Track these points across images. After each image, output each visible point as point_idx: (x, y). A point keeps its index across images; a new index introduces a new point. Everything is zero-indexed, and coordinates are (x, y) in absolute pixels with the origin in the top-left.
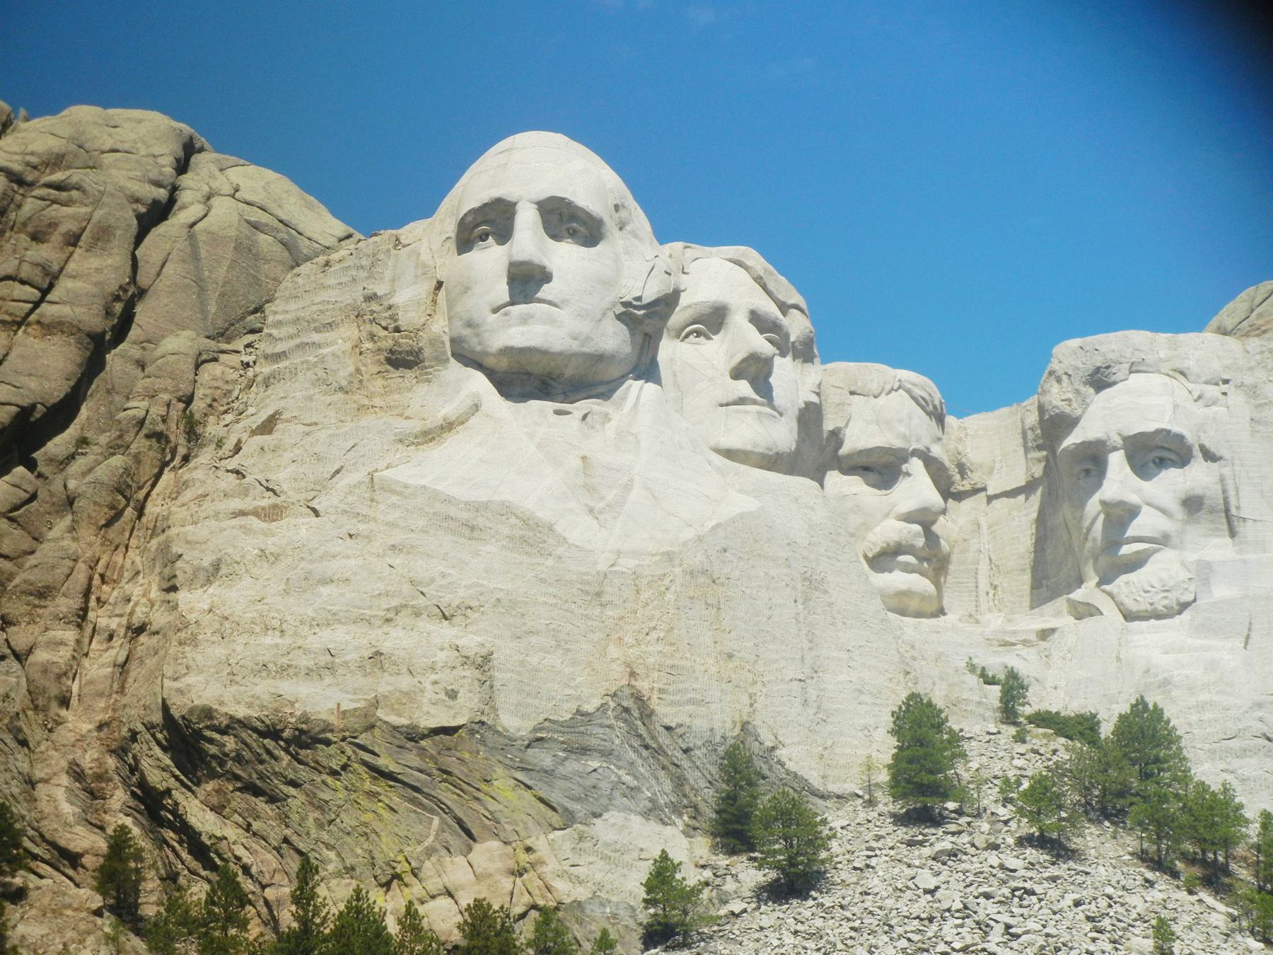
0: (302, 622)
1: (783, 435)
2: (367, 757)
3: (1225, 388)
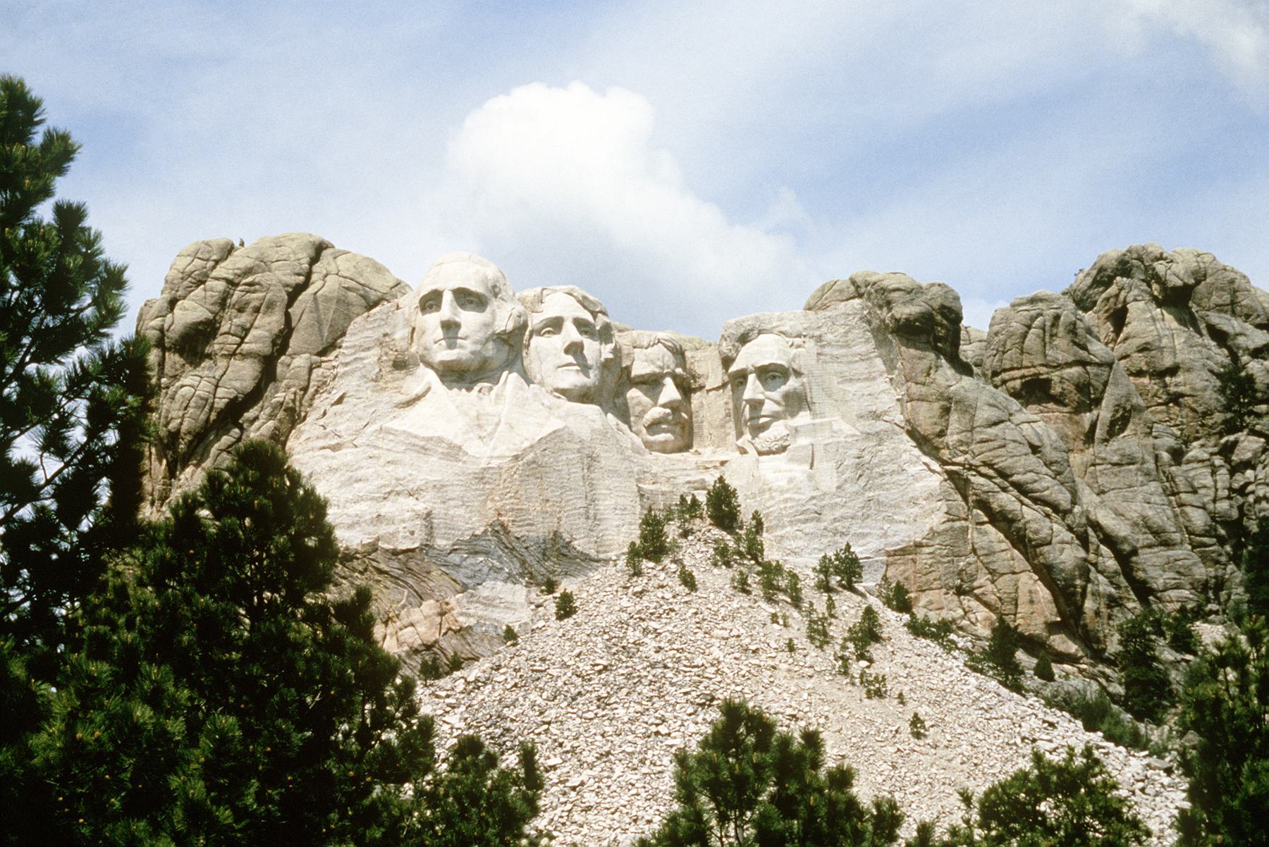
1: (592, 379)
2: (375, 564)
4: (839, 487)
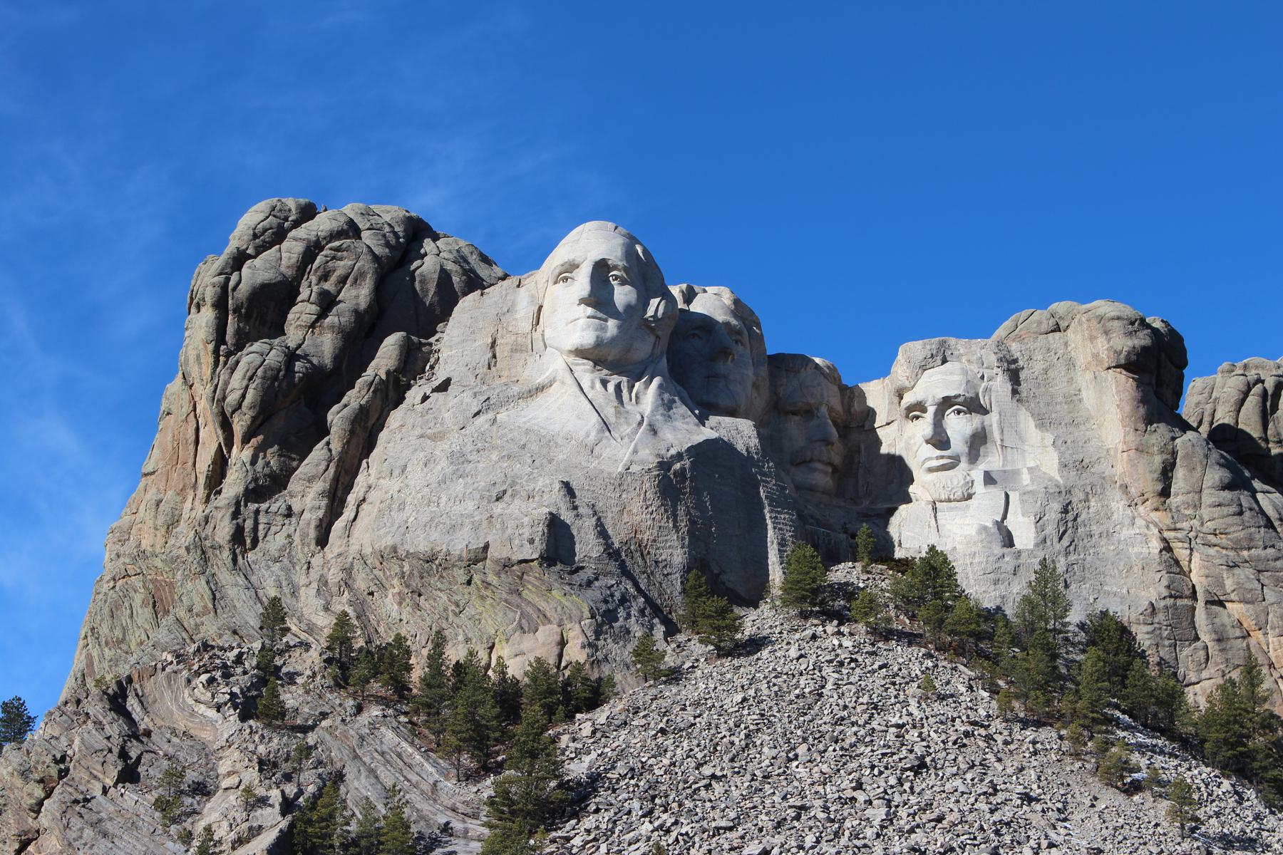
3: (996, 370)
4: (1037, 545)
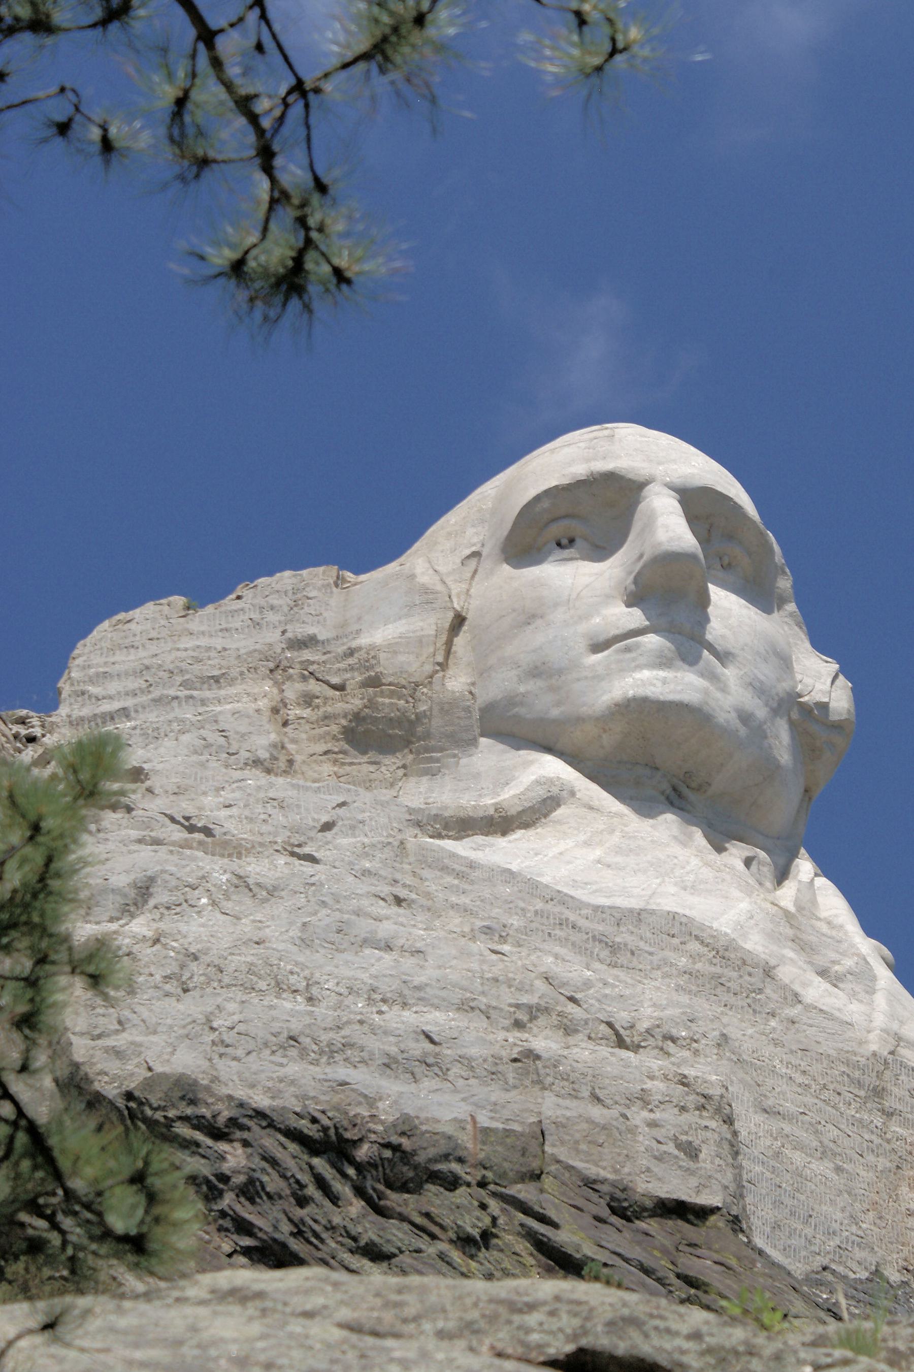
0: (351, 990)
